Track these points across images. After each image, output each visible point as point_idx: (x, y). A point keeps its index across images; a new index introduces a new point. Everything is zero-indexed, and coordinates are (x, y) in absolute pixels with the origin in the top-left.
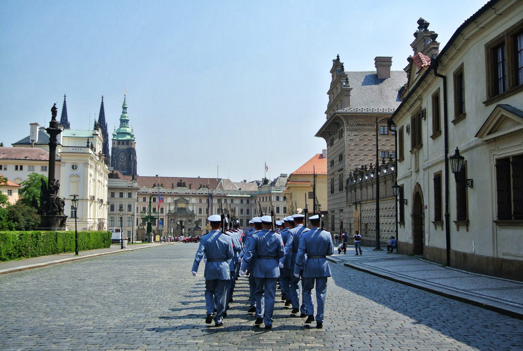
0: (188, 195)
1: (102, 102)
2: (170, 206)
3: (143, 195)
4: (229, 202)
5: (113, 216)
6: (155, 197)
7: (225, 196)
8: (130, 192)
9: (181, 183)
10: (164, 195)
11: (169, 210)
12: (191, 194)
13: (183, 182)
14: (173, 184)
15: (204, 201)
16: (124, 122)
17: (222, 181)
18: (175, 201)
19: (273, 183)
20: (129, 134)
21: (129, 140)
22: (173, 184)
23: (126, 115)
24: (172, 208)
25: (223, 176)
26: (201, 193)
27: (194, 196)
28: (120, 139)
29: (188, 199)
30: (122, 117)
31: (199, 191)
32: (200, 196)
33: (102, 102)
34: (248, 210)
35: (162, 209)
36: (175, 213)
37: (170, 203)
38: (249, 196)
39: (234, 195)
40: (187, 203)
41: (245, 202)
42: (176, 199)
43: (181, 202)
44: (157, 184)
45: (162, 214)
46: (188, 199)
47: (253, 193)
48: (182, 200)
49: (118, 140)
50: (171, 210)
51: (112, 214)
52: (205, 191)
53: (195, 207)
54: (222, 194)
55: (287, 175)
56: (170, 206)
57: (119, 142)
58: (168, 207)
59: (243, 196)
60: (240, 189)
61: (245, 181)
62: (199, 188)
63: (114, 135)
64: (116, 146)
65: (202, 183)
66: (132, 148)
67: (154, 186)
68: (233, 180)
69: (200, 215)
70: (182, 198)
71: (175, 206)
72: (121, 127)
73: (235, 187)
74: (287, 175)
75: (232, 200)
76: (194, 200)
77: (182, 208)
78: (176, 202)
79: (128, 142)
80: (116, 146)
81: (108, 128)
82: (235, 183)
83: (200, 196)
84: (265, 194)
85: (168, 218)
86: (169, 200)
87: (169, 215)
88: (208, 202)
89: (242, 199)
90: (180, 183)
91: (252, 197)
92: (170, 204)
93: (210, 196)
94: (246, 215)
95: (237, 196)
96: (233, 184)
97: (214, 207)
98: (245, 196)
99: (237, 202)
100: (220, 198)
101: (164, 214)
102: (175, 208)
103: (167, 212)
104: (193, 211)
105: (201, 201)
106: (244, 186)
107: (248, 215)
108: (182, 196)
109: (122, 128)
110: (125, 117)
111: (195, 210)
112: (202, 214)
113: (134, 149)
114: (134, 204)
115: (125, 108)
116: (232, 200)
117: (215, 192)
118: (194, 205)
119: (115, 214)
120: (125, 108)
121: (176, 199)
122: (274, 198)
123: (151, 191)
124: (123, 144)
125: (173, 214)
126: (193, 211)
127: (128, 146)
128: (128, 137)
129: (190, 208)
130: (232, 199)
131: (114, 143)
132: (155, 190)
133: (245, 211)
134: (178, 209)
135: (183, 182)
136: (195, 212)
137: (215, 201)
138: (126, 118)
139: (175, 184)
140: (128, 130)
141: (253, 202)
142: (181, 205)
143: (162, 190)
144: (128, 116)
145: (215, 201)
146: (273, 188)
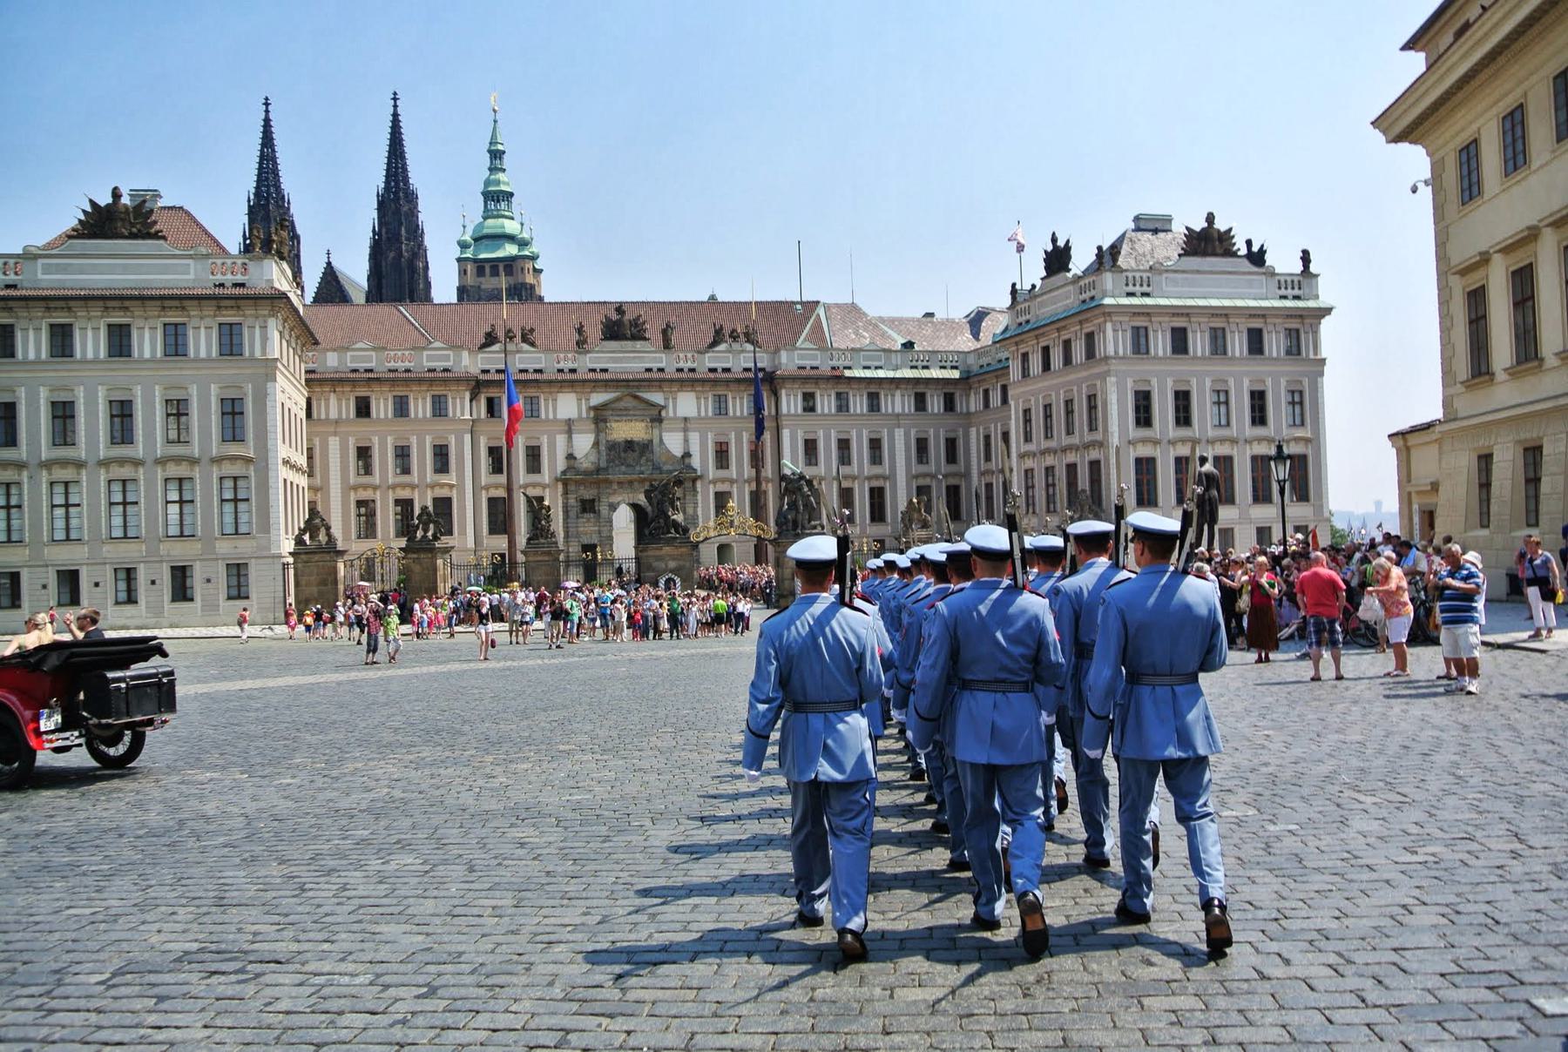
0: (657, 380)
1: (395, 115)
2: (570, 432)
3: (431, 382)
4: (858, 404)
5: (126, 472)
6: (493, 392)
7: (839, 379)
8: (230, 317)
9: (621, 325)
10: (535, 383)
11: (570, 457)
12: (670, 373)
13: (628, 317)
14: (580, 330)
15: (740, 405)
16: (496, 198)
17: (821, 311)
18: (595, 408)
19: (1107, 257)
20: (511, 238)
21: (514, 259)
22: (580, 330)
23: (501, 176)
24: (583, 443)
25: (824, 290)
26: (719, 365)
27: (688, 381)
28: (482, 256)
29: (657, 397)
30: (487, 183)
31: (709, 361)
32: (715, 383)
33: (395, 115)
34: (951, 444)
35: (534, 455)
36: (598, 470)
37: (569, 422)
38: (956, 374)
39: (881, 374)
40: (657, 417)
41: (935, 404)
42: (598, 398)
43: (624, 414)
44: (501, 334)
45: (534, 478)
46: (657, 397)
47: (971, 360)
48: (629, 403)
49: (475, 261)
50: (579, 454)
51: (122, 461)
52: (738, 358)
53: (694, 438)
54: (825, 370)
55: (1168, 220)
56: (570, 432)
57: (480, 266)
58: (561, 440)
59: (925, 374)
60: (909, 345)
61: (930, 315)
62: (714, 344)
63: (463, 246)
64: (471, 279)
65: (725, 323)
66: (524, 285)
67: (491, 339)
68: (873, 309)
69: (723, 473)
70: (631, 392)
71: (598, 432)
72: (485, 218)
73: (884, 335)
74: (1168, 220)
75: (874, 399)
76: (686, 404)
77: (629, 445)
78: (600, 416)
79: (510, 264)
80: (471, 279)
81: (422, 205)
82: (882, 320)
83: (715, 382)
84: (1059, 323)
85: (566, 493)
86: (567, 406)
87: (571, 478)
88: (758, 408)
89: (919, 391)
90: (619, 323)
91: (966, 380)
92: (569, 427)
93: (765, 383)
94: (945, 468)
95: (899, 374)
96: (874, 325)
97: (786, 433)
98: (935, 373)
99: (898, 403)
100: (810, 382)
101: (546, 476)
102: (596, 444)
103: (561, 465)
104: (687, 455)
105: (721, 409)
106: (928, 331)
107: (952, 468)
108: (630, 386)
109: (490, 222)
110: (498, 182)
111: (695, 449)
112: (733, 472)
113: (532, 287)
114: (262, 398)
115: (496, 155)
116: (874, 399)
117: (788, 362)
118: (687, 429)
119: (137, 463)
120: (496, 155)
121: (598, 398)
122: (1114, 341)
123: (470, 363)
124: (495, 273)
125: (586, 473)
126: (687, 455)
127: (512, 280)
128: (511, 250)
129: (673, 443)
130: (874, 390)
131: (463, 273)
132: (491, 360)
133: (937, 450)
134: (612, 446)
135: (628, 317)
136: (696, 462)
137: (790, 403)
138: (503, 188)
139: (594, 331)
140: (511, 227)
141: (974, 403)
142: (627, 430)
143: (525, 359)
144: (506, 182)
145: (790, 403)
146: (1108, 279)
